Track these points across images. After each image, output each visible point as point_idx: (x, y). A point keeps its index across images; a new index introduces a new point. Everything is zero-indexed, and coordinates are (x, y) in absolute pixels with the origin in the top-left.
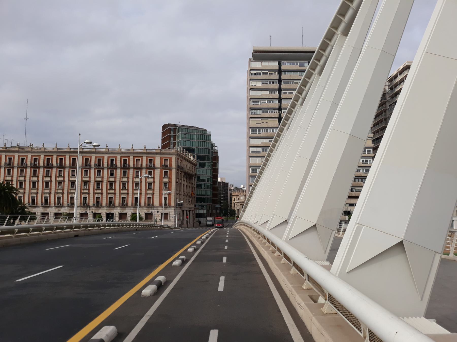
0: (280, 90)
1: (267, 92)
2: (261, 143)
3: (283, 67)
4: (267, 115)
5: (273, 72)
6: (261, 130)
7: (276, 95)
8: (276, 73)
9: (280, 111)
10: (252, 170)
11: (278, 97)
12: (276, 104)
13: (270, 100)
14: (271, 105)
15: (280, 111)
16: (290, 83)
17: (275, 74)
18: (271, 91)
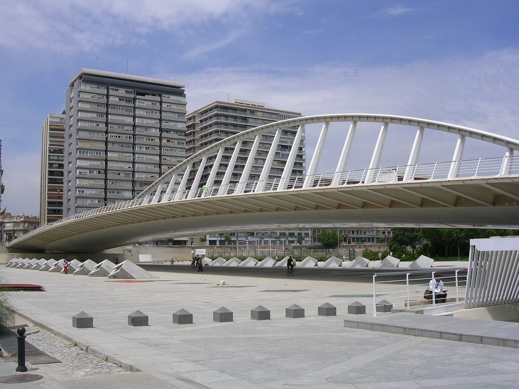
0: (107, 114)
1: (95, 115)
2: (88, 165)
3: (111, 92)
4: (95, 136)
5: (101, 97)
6: (89, 152)
7: (104, 119)
8: (105, 97)
9: (107, 135)
10: (79, 191)
11: (105, 121)
12: (102, 126)
13: (98, 123)
14: (98, 128)
15: (107, 135)
16: (117, 109)
17: (103, 98)
18: (99, 113)
